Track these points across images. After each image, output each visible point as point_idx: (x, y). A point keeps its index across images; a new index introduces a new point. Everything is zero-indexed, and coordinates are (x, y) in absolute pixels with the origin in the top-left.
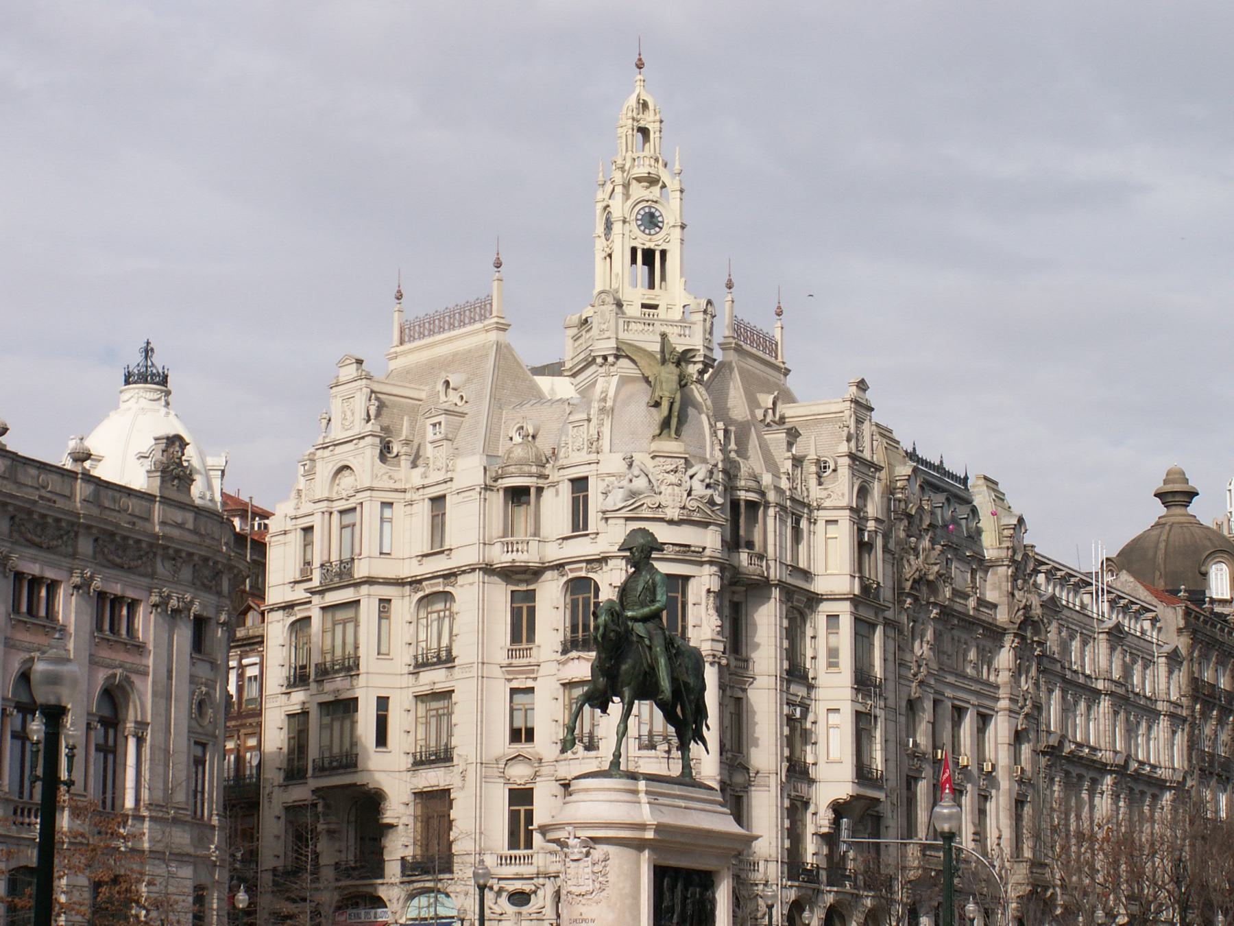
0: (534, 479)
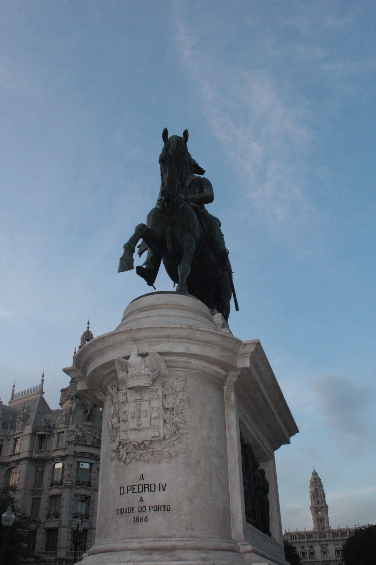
0: (47, 432)
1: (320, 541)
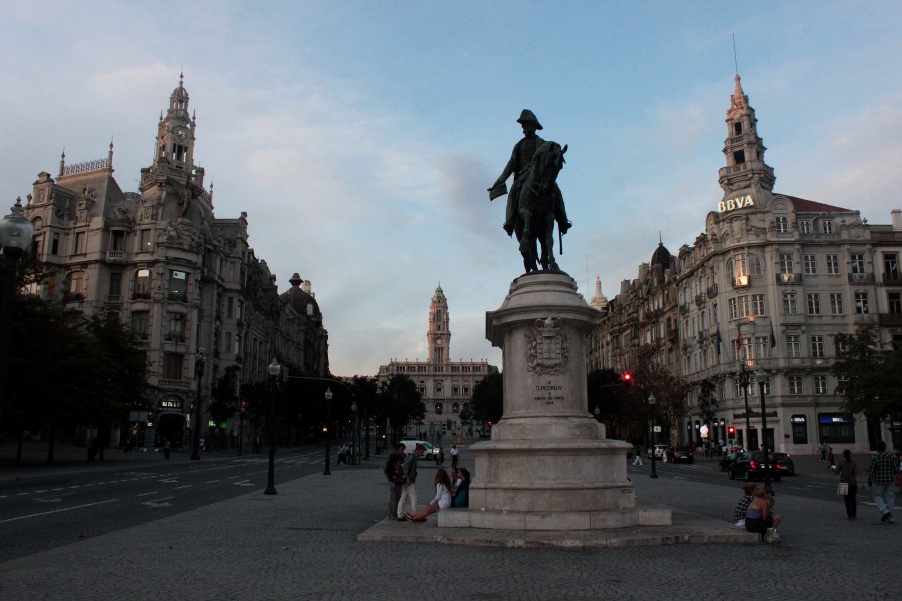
1: (434, 376)
